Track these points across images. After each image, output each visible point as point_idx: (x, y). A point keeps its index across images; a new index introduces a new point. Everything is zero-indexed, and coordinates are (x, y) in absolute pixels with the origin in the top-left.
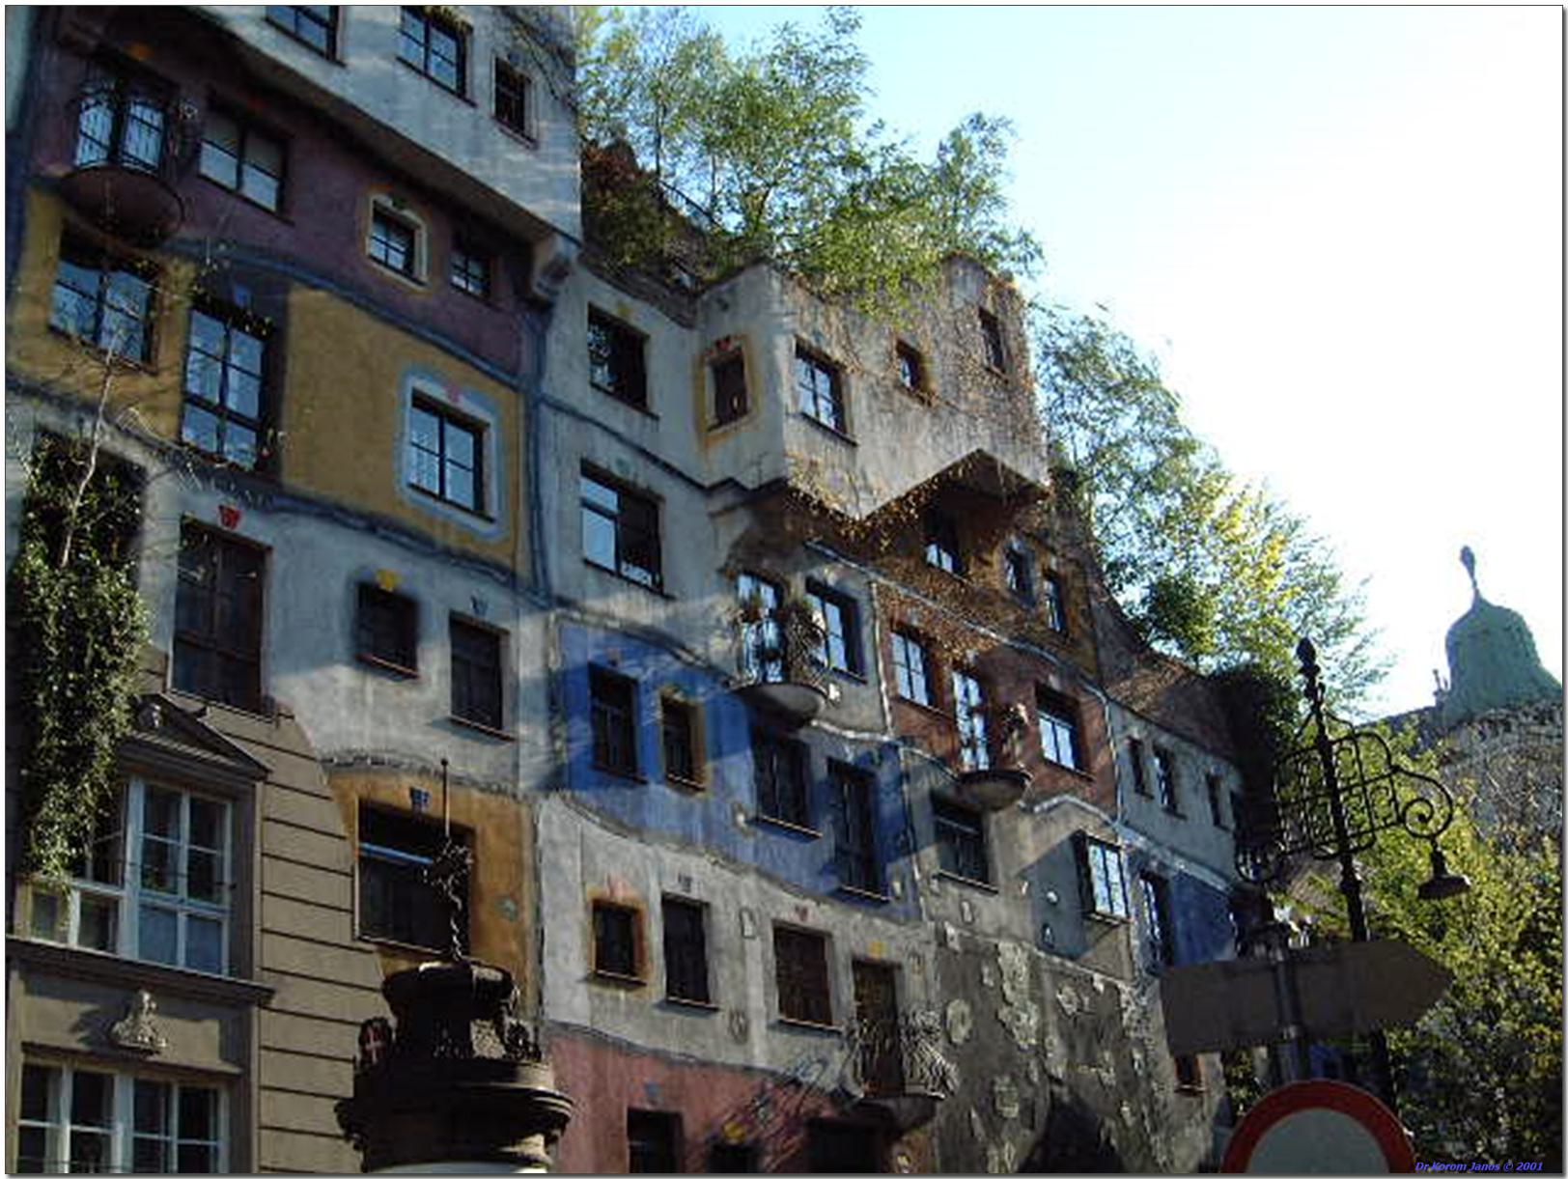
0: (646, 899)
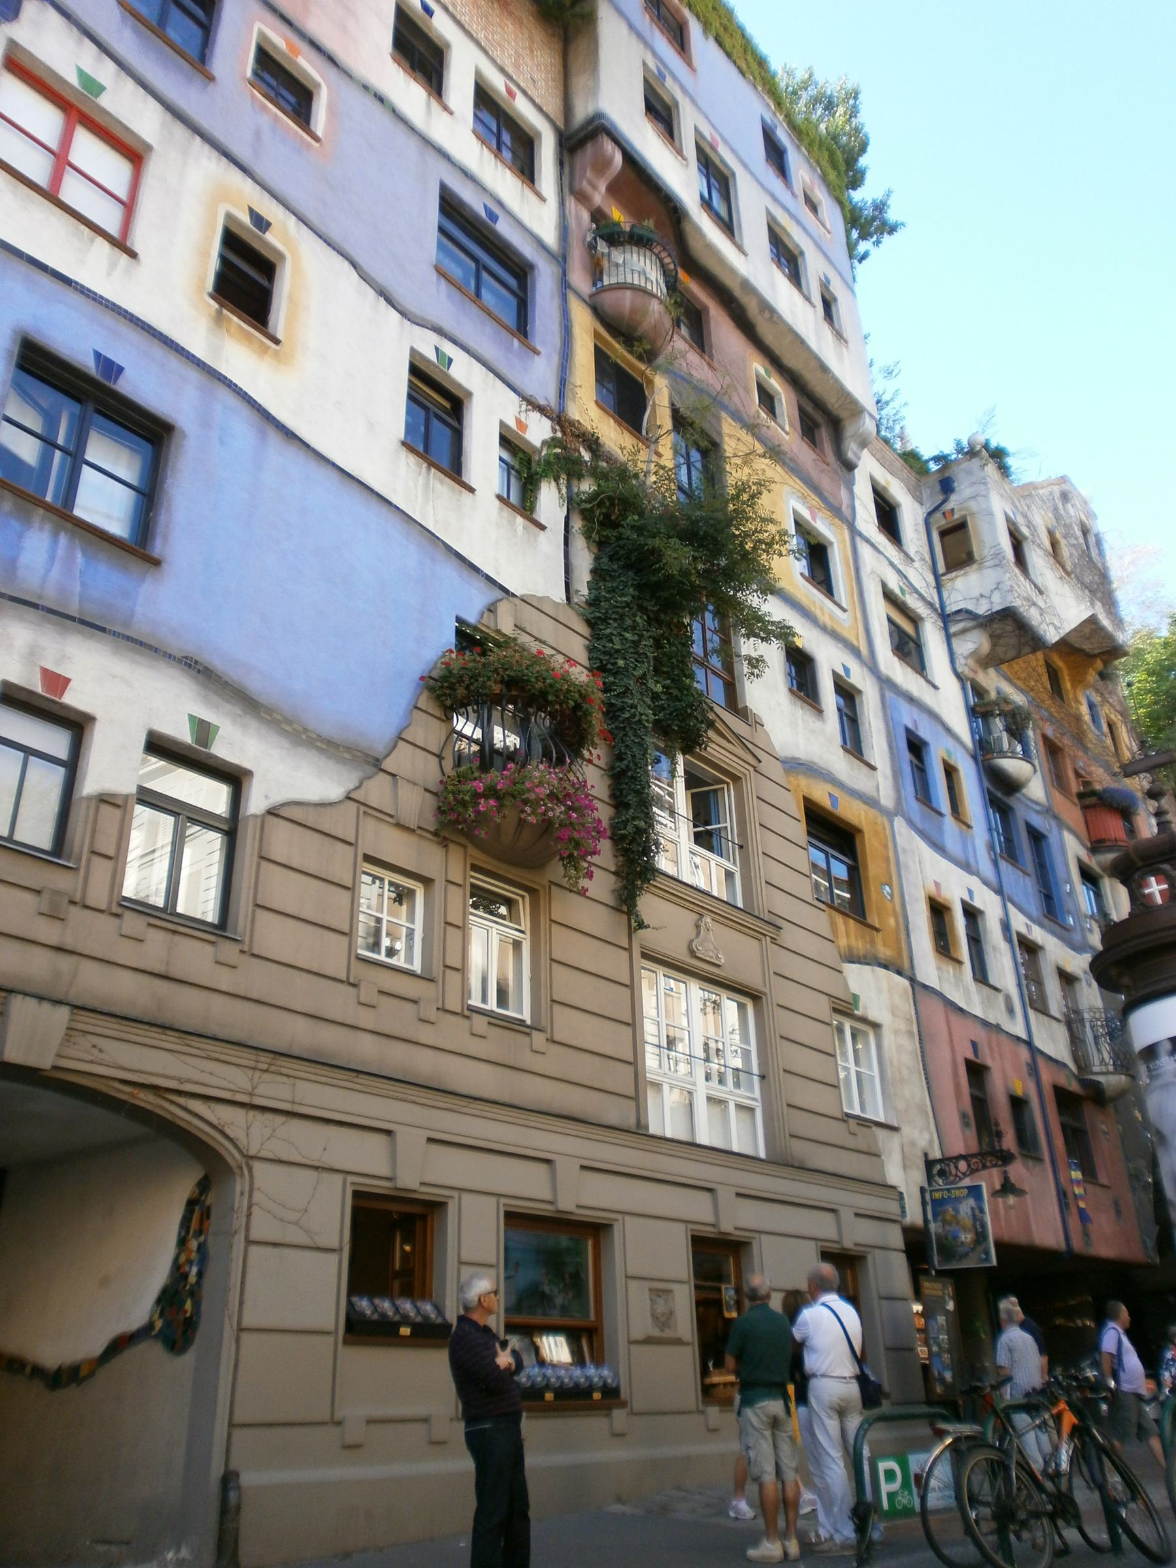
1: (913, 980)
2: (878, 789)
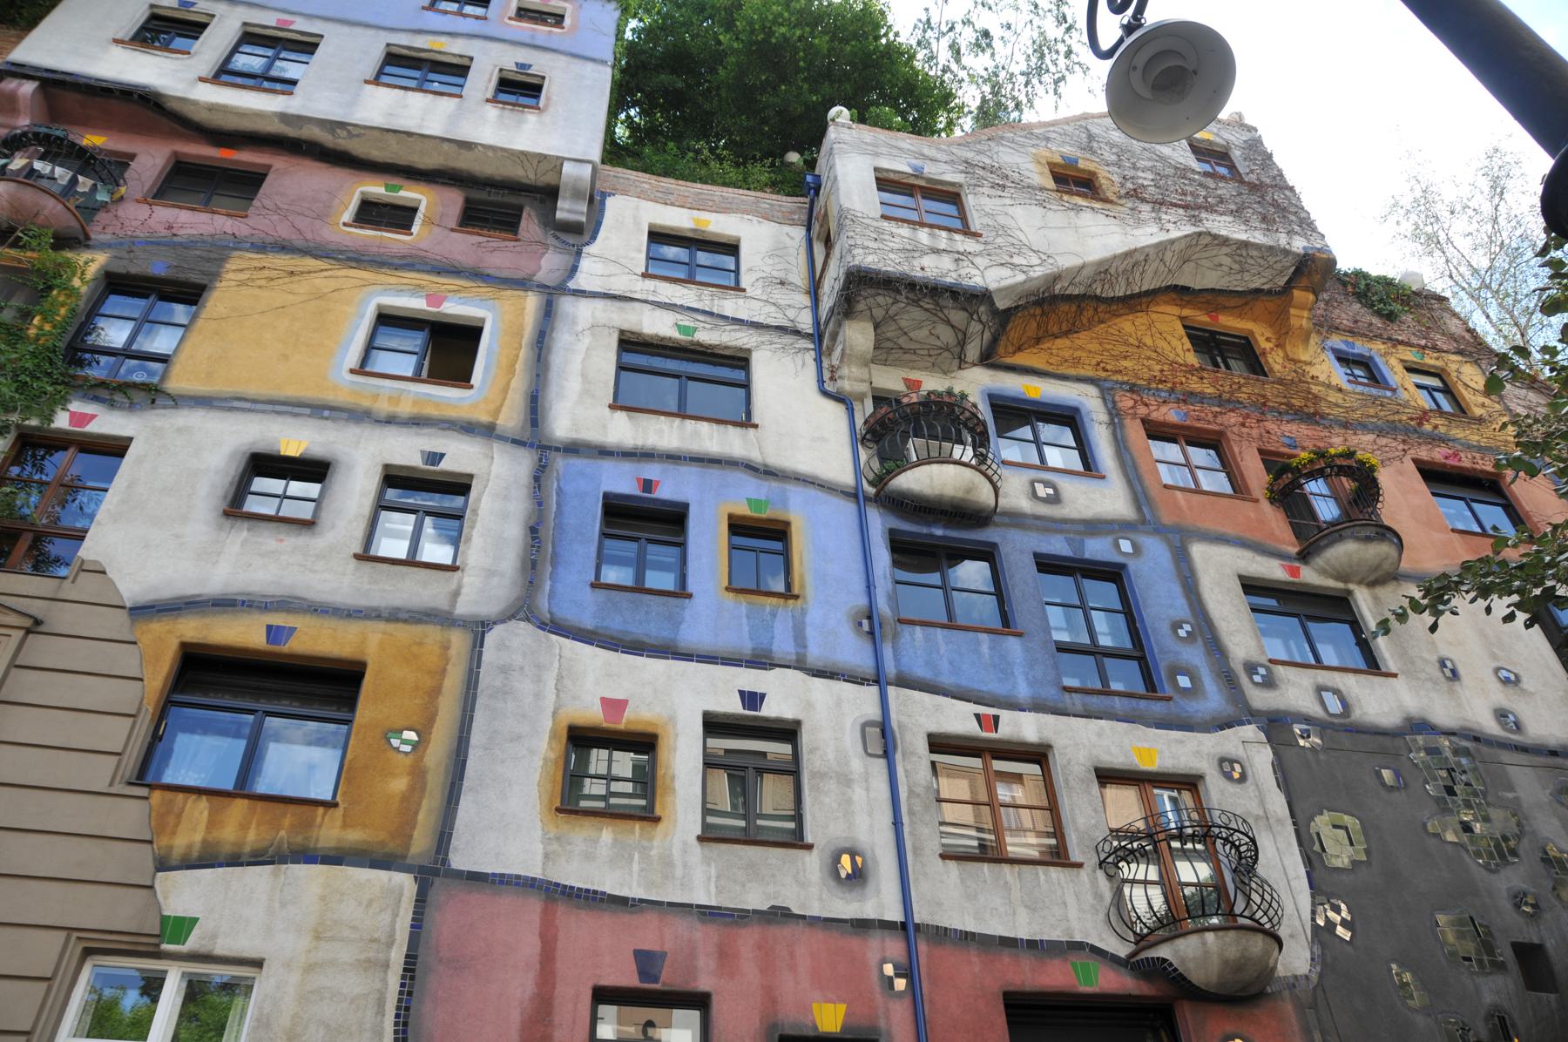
0: (672, 720)
1: (433, 873)
2: (456, 594)
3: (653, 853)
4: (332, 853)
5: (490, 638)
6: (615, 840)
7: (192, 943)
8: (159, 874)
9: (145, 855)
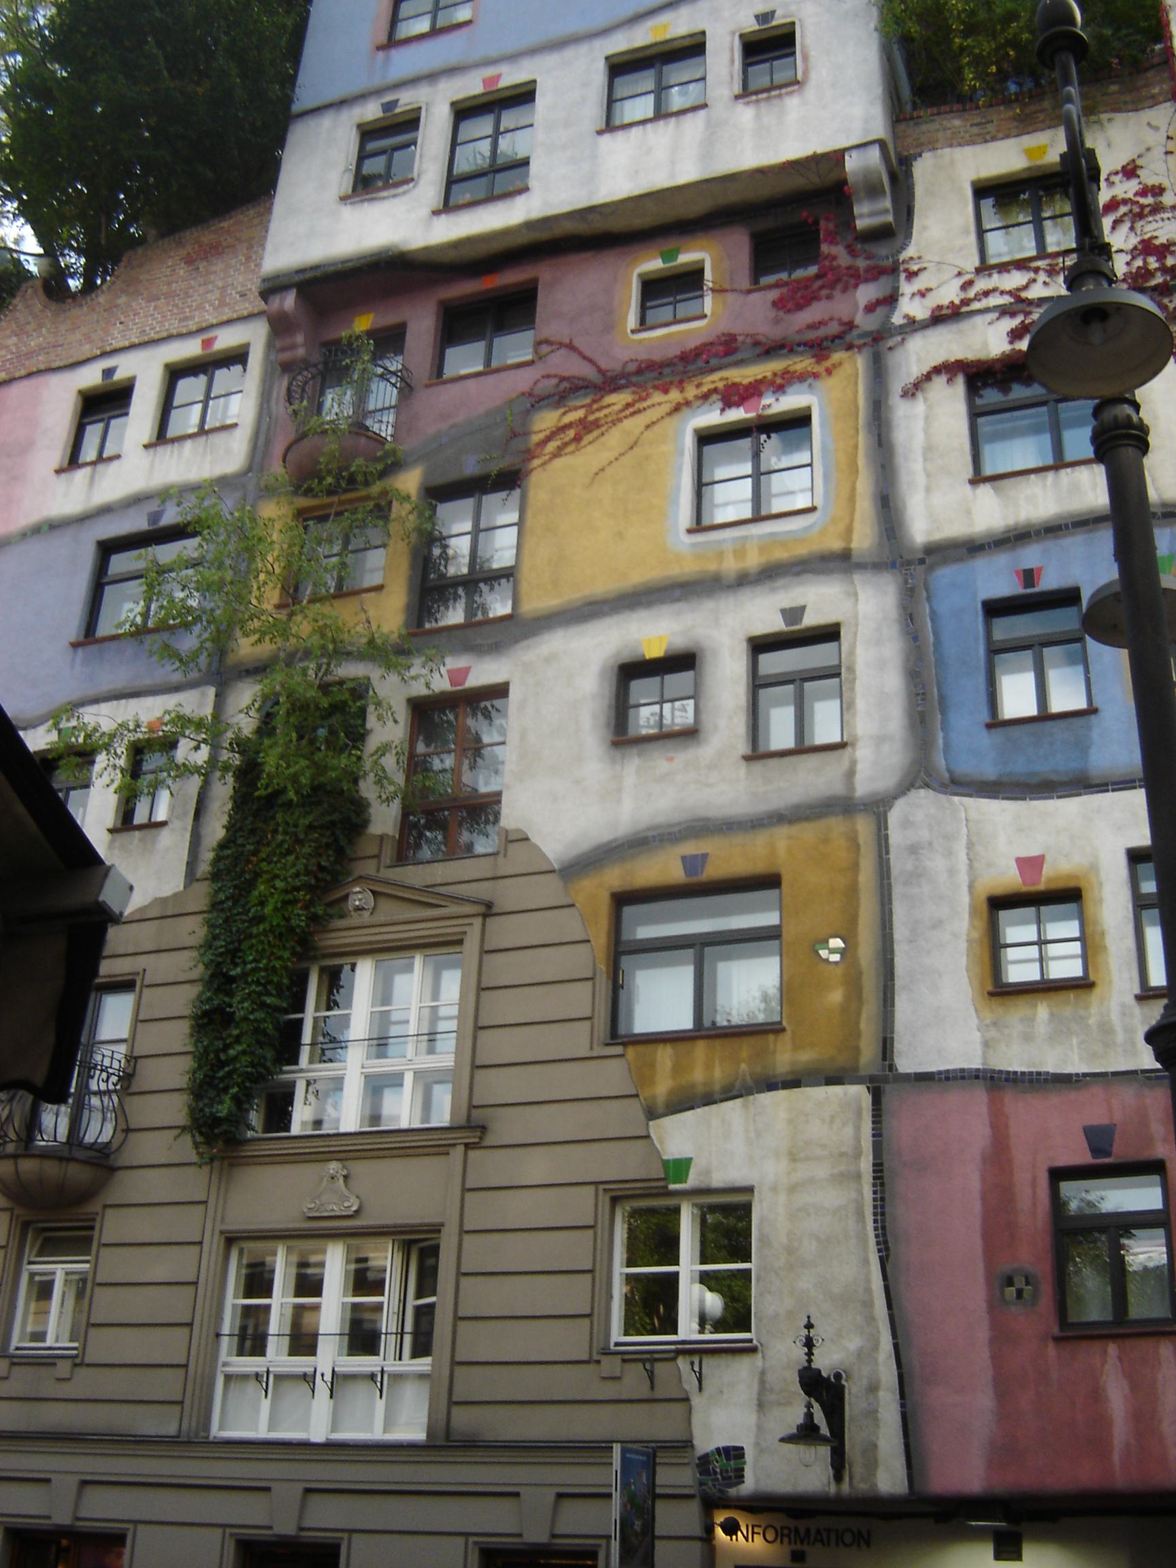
0: (1094, 868)
1: (884, 1083)
2: (851, 774)
3: (1092, 1021)
4: (789, 1078)
5: (894, 817)
6: (1052, 1015)
7: (692, 1181)
8: (651, 1123)
9: (634, 1109)
